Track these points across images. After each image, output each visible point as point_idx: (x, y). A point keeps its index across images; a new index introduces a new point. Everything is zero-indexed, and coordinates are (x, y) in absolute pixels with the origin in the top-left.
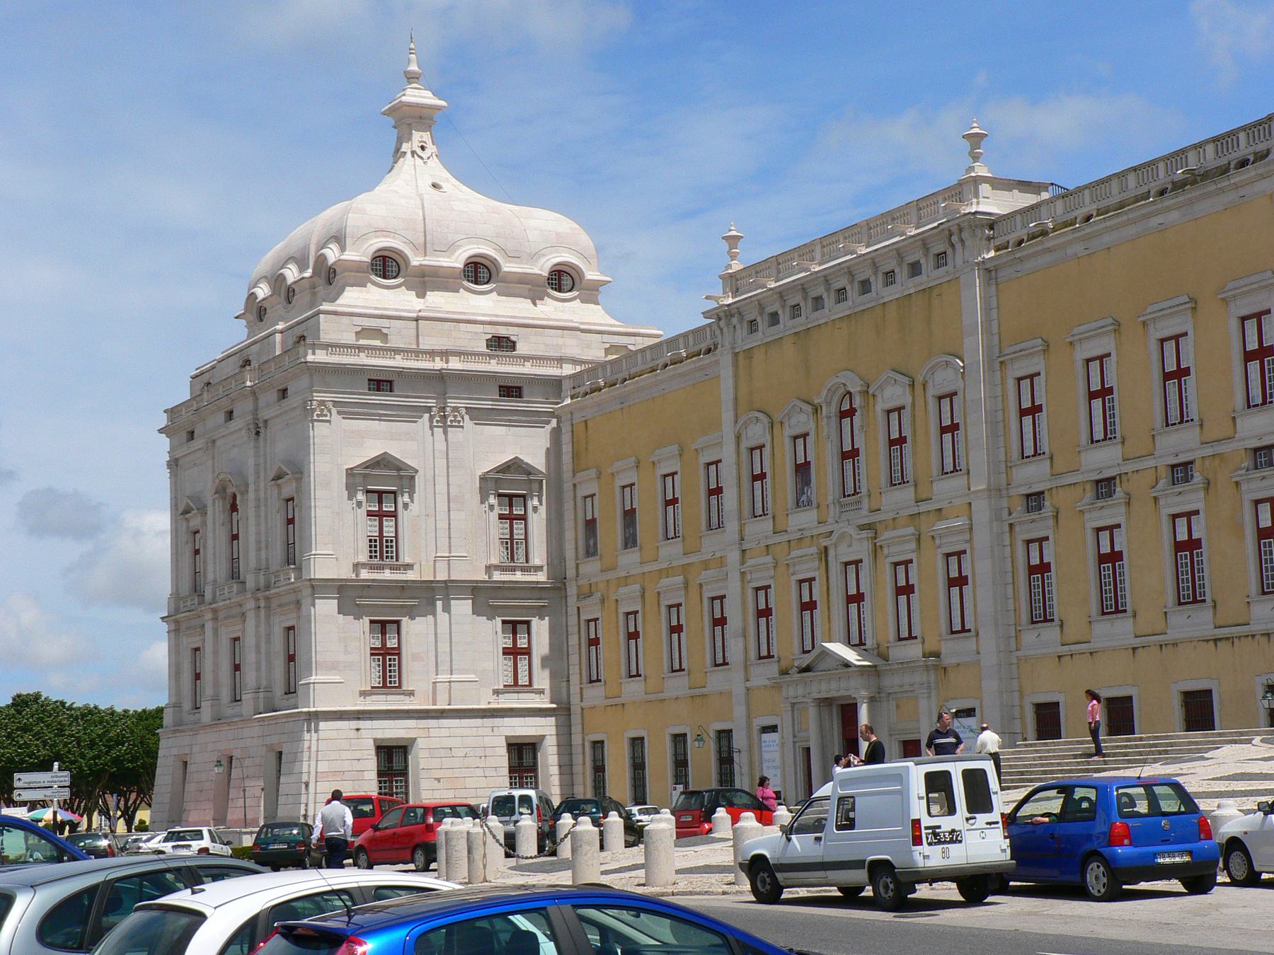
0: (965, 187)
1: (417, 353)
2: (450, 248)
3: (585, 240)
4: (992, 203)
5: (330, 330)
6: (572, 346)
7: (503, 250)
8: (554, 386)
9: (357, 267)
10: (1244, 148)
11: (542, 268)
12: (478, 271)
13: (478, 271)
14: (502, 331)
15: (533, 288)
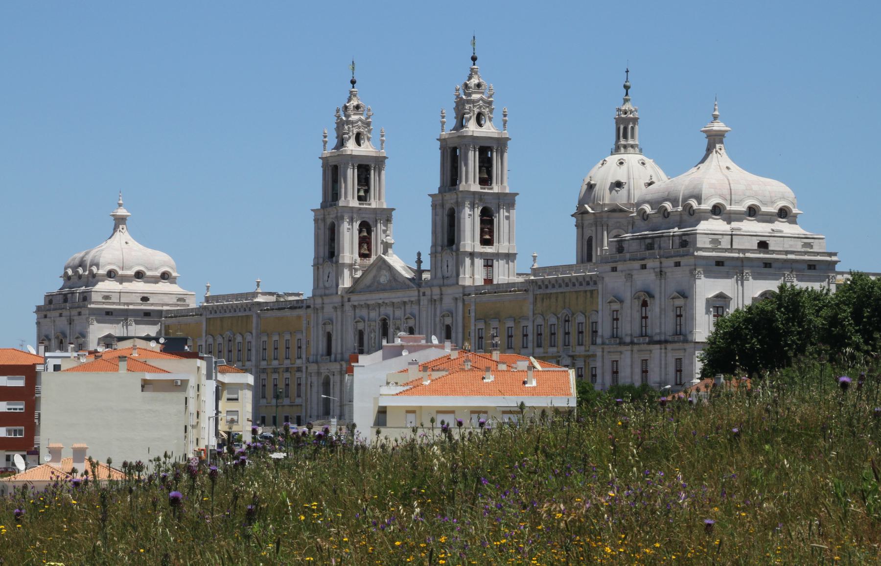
0: (255, 295)
1: (120, 304)
2: (130, 268)
3: (173, 262)
4: (260, 299)
5: (95, 297)
6: (166, 299)
7: (147, 268)
8: (160, 313)
9: (103, 275)
10: (300, 305)
11: (158, 273)
12: (139, 275)
13: (139, 275)
14: (145, 295)
15: (155, 280)
